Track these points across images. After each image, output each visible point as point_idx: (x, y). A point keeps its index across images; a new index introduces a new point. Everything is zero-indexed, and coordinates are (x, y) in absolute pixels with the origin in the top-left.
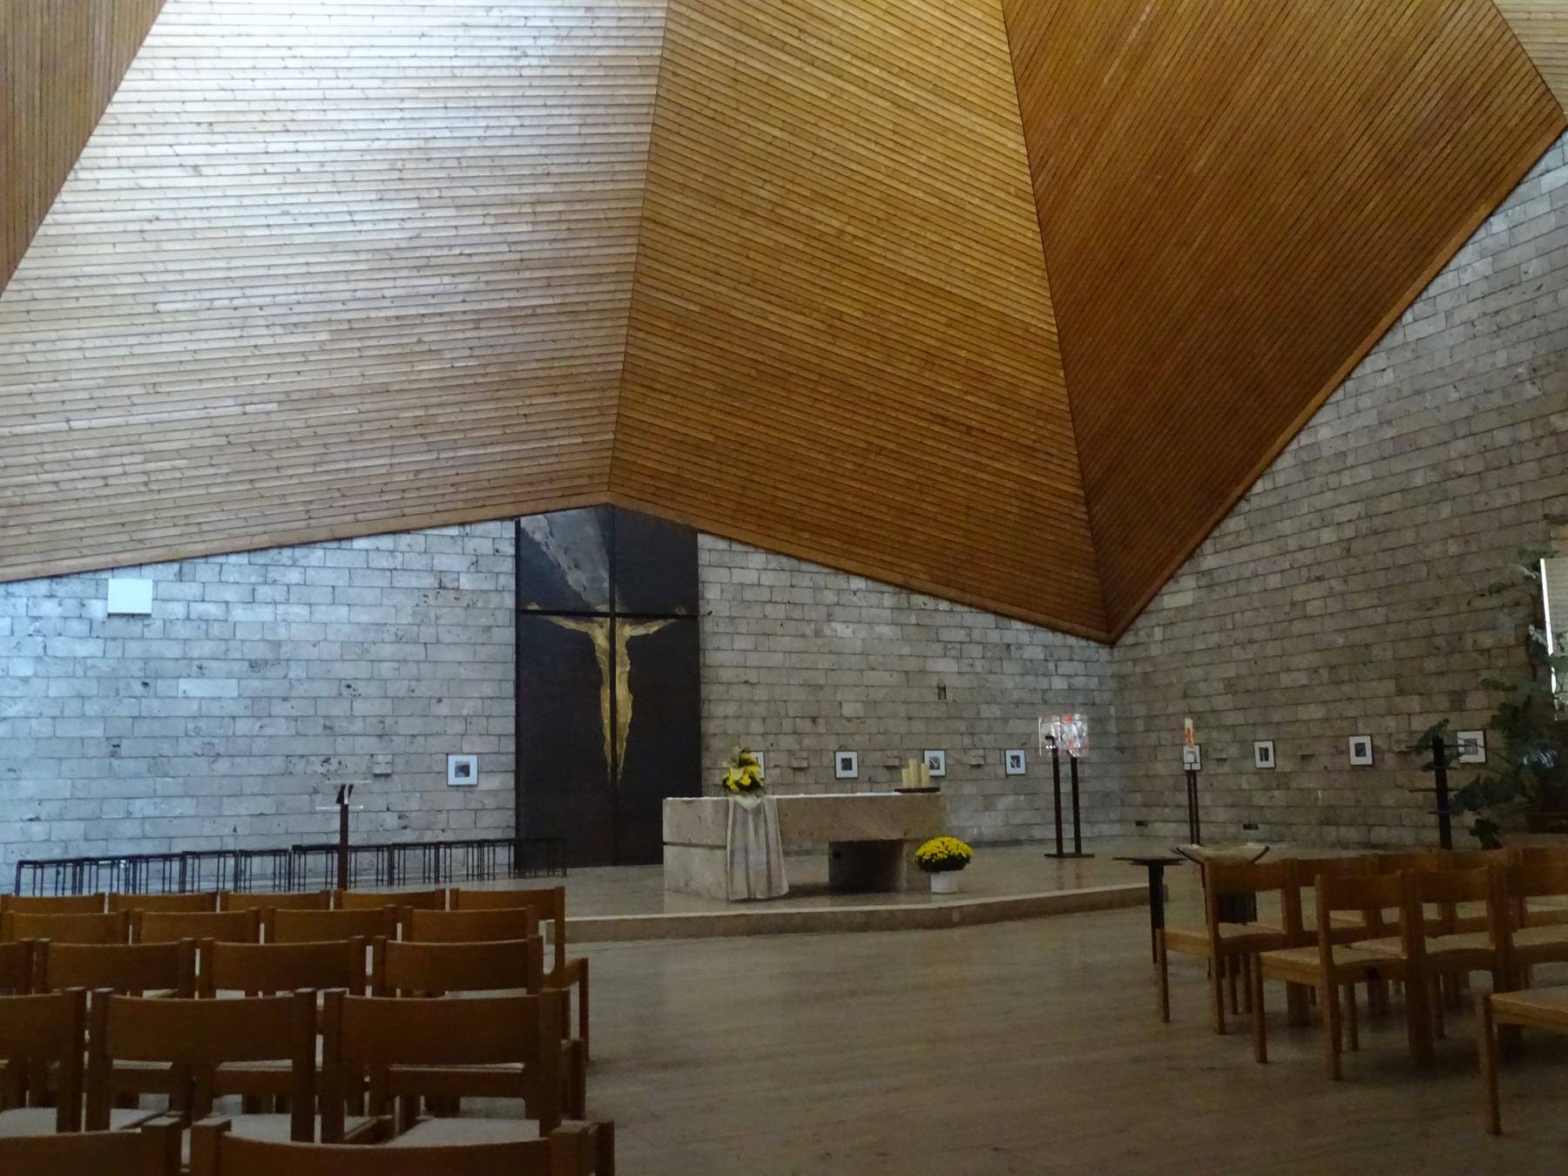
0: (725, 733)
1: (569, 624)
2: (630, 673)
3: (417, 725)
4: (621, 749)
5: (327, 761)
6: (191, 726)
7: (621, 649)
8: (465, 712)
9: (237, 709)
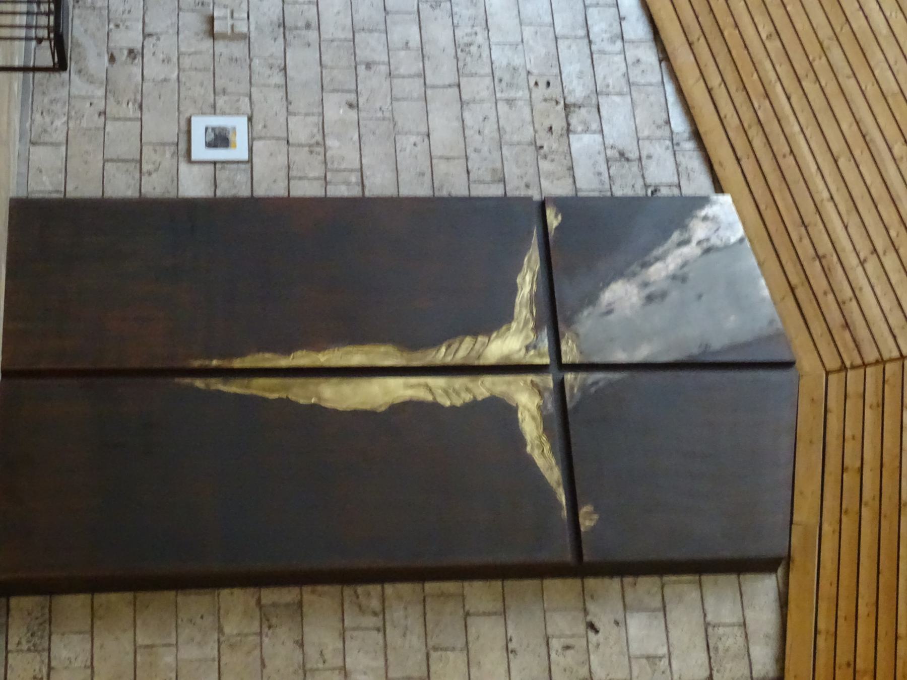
1: (527, 283)
4: (260, 387)
7: (484, 387)
8: (330, 142)
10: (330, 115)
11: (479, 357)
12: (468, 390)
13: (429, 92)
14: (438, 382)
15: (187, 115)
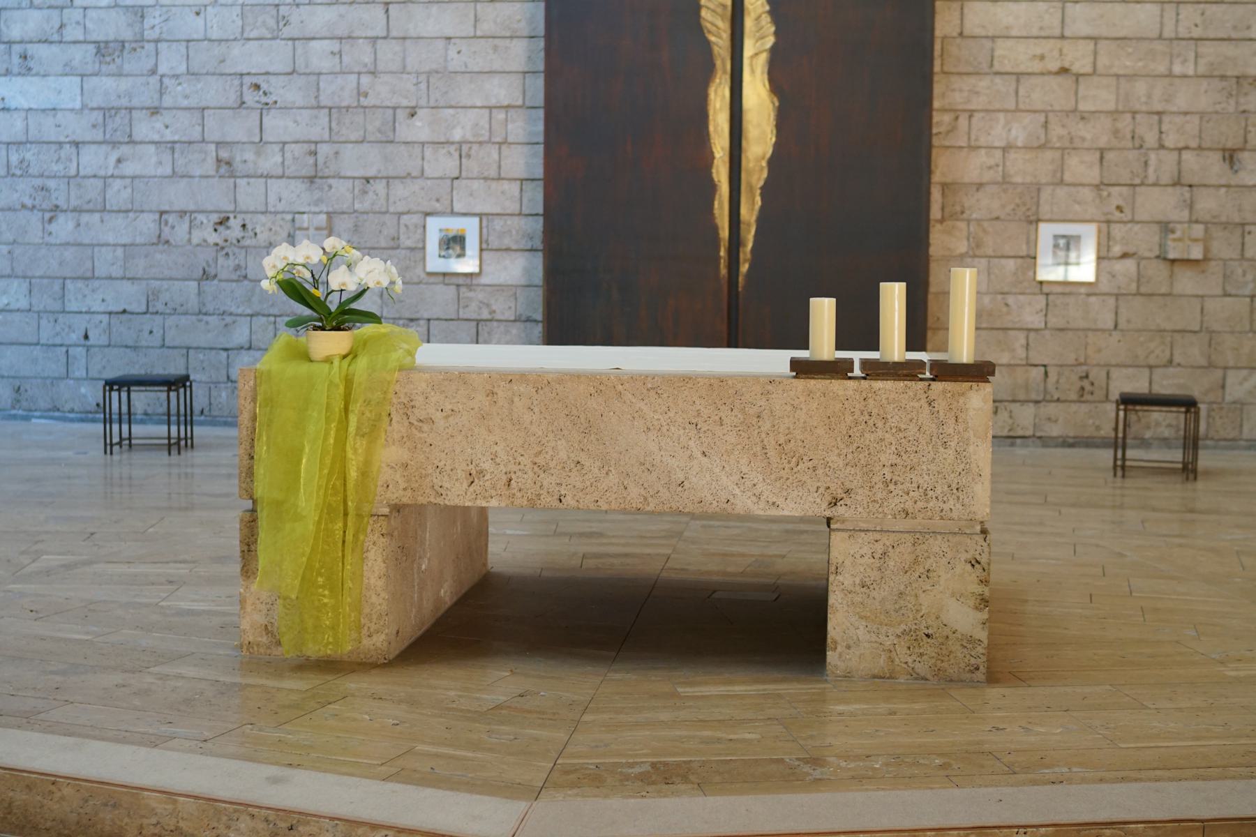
0: (1005, 182)
2: (774, 51)
3: (371, 160)
4: (749, 212)
5: (223, 222)
6: (14, 158)
8: (457, 135)
9: (78, 128)
10: (424, 135)
11: (724, 6)
12: (758, 18)
13: (394, 33)
14: (749, 49)
15: (423, 275)
